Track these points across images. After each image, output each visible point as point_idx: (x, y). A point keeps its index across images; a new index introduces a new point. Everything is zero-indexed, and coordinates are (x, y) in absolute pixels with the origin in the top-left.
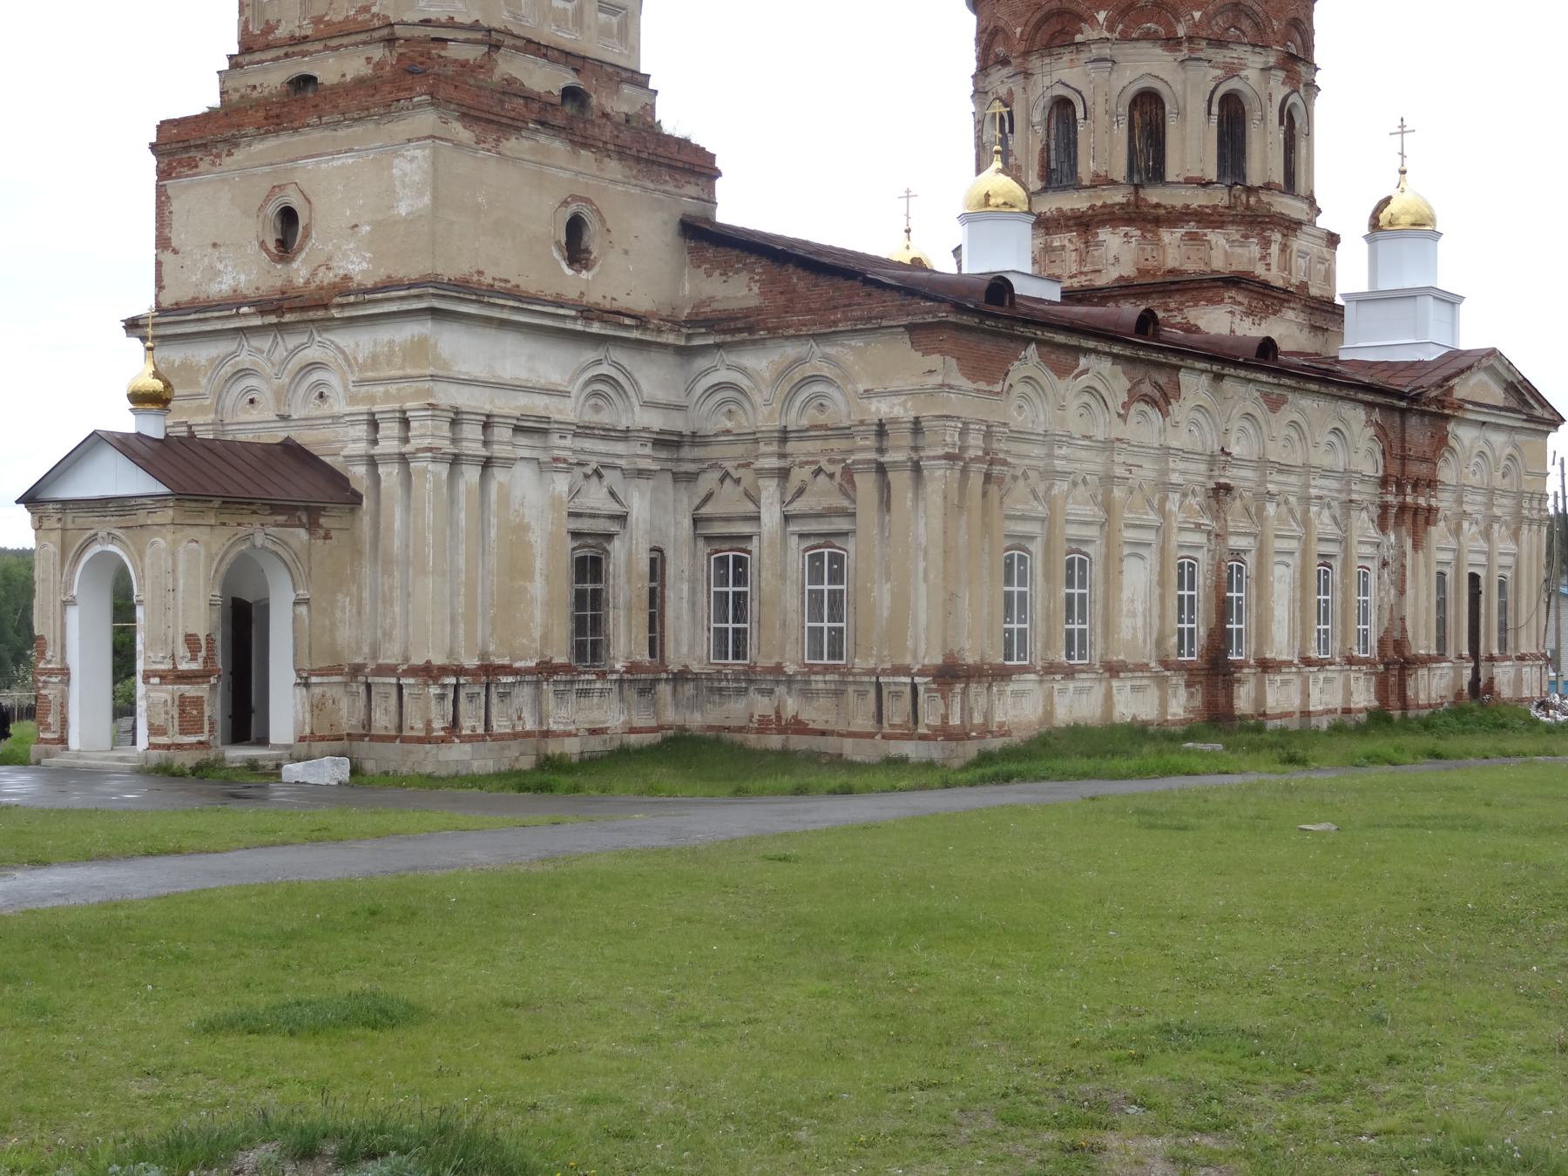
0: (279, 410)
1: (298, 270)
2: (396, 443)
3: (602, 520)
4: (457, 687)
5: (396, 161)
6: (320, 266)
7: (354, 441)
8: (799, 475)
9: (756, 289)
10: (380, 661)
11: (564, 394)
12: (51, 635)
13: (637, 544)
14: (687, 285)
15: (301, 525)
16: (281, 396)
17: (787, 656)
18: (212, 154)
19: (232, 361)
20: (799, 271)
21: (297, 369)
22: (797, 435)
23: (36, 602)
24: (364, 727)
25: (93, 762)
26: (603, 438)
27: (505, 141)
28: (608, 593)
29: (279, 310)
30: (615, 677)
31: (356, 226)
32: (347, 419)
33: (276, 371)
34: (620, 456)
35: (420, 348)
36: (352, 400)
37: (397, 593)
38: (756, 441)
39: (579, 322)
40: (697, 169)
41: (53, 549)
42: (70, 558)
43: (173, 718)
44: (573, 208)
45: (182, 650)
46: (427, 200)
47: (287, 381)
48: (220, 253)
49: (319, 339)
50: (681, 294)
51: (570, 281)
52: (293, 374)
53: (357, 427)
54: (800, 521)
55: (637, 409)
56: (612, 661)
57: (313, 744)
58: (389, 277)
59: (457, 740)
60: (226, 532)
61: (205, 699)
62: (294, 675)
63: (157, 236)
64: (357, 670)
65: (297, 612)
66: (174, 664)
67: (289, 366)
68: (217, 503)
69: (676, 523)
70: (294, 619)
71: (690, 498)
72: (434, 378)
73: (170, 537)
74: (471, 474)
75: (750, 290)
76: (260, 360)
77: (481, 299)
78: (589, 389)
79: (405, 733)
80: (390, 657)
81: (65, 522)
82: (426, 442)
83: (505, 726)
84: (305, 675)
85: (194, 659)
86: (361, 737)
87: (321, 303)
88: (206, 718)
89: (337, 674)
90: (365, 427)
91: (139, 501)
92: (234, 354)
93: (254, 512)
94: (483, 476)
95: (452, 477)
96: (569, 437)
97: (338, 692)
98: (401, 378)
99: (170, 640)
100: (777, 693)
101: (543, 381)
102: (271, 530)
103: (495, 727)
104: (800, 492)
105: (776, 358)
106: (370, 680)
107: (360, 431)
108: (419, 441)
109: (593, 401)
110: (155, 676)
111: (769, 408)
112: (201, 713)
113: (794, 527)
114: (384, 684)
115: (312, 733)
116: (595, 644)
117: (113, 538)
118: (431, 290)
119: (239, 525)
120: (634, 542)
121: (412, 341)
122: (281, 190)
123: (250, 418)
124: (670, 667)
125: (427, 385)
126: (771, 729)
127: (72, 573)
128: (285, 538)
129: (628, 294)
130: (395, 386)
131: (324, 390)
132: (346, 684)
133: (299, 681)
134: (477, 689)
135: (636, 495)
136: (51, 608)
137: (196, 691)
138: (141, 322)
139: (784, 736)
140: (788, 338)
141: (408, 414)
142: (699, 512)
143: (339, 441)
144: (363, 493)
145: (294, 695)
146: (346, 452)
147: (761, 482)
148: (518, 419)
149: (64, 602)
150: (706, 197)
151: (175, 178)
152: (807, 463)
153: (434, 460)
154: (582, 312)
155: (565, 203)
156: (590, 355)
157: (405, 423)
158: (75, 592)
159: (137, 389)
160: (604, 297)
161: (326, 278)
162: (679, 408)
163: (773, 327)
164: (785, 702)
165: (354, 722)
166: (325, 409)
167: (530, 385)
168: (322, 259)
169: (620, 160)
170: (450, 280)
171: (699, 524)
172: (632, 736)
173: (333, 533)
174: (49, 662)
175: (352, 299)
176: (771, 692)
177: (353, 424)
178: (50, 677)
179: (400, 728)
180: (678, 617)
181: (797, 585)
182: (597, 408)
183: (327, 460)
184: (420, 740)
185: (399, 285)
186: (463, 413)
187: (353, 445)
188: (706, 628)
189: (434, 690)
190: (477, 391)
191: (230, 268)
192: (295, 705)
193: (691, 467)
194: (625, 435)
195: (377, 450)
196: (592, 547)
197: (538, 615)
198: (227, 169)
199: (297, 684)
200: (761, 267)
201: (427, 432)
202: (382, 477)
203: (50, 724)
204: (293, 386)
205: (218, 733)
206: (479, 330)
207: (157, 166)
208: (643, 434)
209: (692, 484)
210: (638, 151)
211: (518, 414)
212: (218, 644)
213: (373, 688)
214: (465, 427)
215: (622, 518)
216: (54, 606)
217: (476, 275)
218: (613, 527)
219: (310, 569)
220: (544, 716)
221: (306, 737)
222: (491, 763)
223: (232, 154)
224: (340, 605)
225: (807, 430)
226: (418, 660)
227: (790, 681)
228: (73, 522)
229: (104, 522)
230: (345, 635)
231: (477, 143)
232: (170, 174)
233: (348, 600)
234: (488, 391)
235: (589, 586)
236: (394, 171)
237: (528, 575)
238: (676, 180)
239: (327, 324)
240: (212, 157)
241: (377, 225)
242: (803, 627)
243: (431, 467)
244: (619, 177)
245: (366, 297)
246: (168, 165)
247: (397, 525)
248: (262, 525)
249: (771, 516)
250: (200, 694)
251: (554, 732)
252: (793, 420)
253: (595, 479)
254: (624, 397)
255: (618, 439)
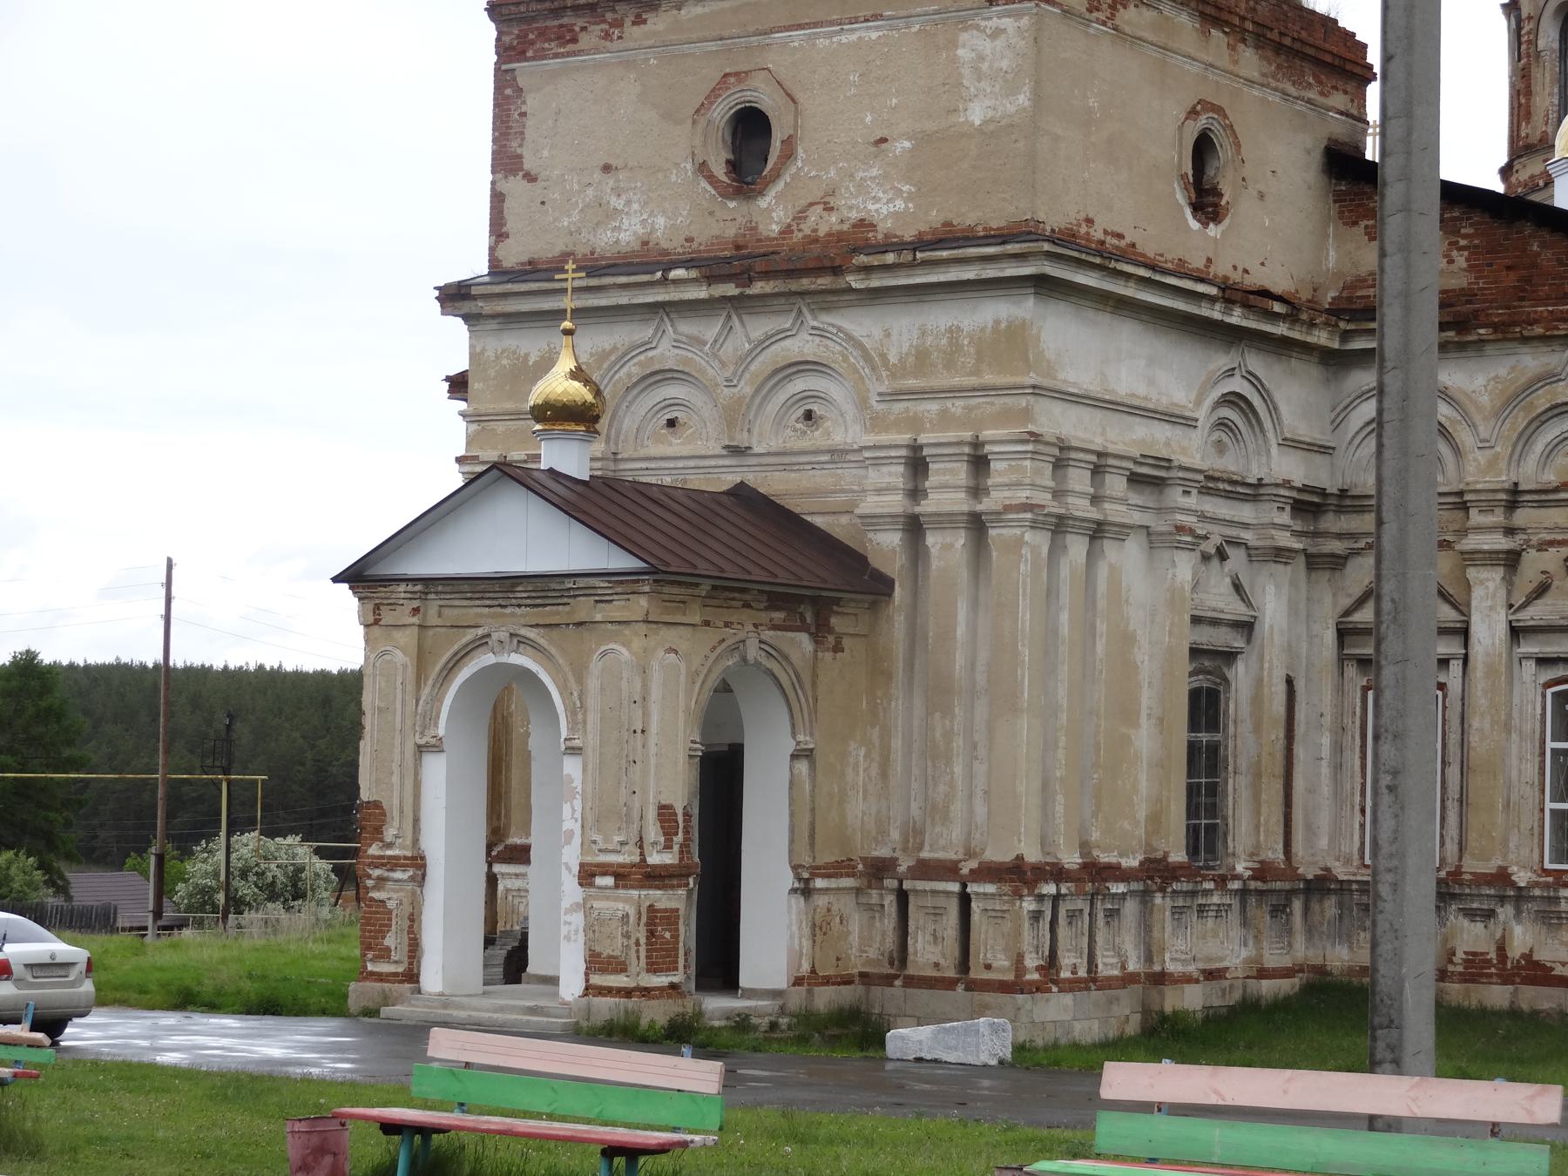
0: (732, 439)
1: (769, 210)
2: (963, 495)
3: (1224, 630)
4: (1057, 898)
5: (964, 37)
6: (811, 204)
7: (879, 491)
8: (1534, 565)
9: (1461, 260)
10: (925, 854)
11: (1188, 422)
12: (396, 802)
13: (1270, 669)
14: (1332, 253)
15: (803, 628)
16: (733, 415)
17: (1511, 856)
18: (604, 21)
19: (642, 357)
20: (1546, 235)
21: (770, 369)
22: (1536, 497)
23: (365, 747)
24: (891, 964)
25: (487, 1015)
26: (1228, 496)
27: (1122, 10)
28: (1226, 747)
29: (744, 276)
30: (1236, 885)
31: (884, 140)
32: (867, 454)
33: (728, 374)
34: (1246, 526)
35: (1014, 340)
36: (876, 423)
37: (959, 743)
38: (1464, 507)
39: (1218, 306)
40: (1349, 67)
41: (401, 658)
42: (433, 675)
43: (637, 944)
44: (1202, 122)
45: (653, 833)
46: (1023, 99)
47: (748, 390)
48: (618, 181)
49: (815, 324)
50: (1324, 268)
52: (761, 378)
53: (885, 469)
54: (1540, 637)
55: (1274, 450)
56: (1230, 860)
57: (817, 989)
58: (947, 224)
59: (1055, 989)
60: (711, 636)
61: (681, 913)
62: (790, 875)
63: (494, 153)
64: (879, 870)
65: (796, 772)
66: (642, 854)
67: (753, 368)
68: (705, 588)
69: (1311, 637)
70: (791, 783)
71: (1334, 595)
72: (1037, 390)
73: (637, 644)
74: (1077, 547)
75: (1451, 262)
76: (698, 359)
77: (1106, 263)
78: (1215, 417)
79: (972, 975)
80: (944, 849)
81: (425, 615)
82: (1022, 495)
83: (1111, 965)
84: (806, 875)
85: (668, 846)
86: (888, 980)
87: (827, 263)
88: (681, 944)
89: (848, 875)
90: (901, 469)
91: (582, 582)
92: (646, 346)
93: (747, 605)
94: (1092, 557)
95: (1056, 550)
96: (1194, 492)
97: (846, 904)
98: (974, 390)
99: (636, 816)
100: (1502, 917)
101: (1164, 400)
102: (768, 635)
103: (1100, 966)
104: (1542, 590)
105: (1502, 372)
106: (907, 885)
107: (890, 474)
108: (1007, 494)
109: (1217, 435)
110: (604, 874)
111: (1488, 453)
112: (675, 937)
113: (1530, 647)
114: (934, 892)
115: (813, 971)
116: (1211, 829)
117: (521, 642)
118: (1047, 247)
119: (727, 625)
120: (1266, 665)
121: (995, 329)
122: (740, 81)
123: (669, 451)
124: (1300, 871)
125: (1023, 401)
126: (1490, 975)
127: (437, 699)
128: (786, 649)
129: (1263, 264)
130: (960, 403)
131: (815, 407)
132: (858, 891)
133: (797, 885)
135: (1271, 589)
136: (397, 757)
137: (670, 899)
138: (474, 291)
139: (1511, 988)
140: (1525, 340)
141: (926, 452)
142: (1350, 619)
143: (843, 491)
144: (895, 576)
145: (789, 901)
146: (864, 509)
147: (1472, 573)
148: (1136, 462)
149: (419, 746)
150: (1355, 112)
151: (533, 59)
152: (1552, 543)
153: (1035, 525)
154: (1223, 290)
155: (1193, 113)
156: (1222, 360)
157: (979, 462)
158: (441, 732)
159: (552, 397)
160: (1235, 268)
161: (823, 223)
162: (1325, 450)
163: (1503, 324)
164: (1512, 931)
165: (872, 953)
166: (816, 439)
167: (1151, 406)
168: (817, 194)
169: (1257, 47)
170: (1053, 231)
171: (1348, 639)
172: (1265, 983)
173: (846, 642)
174: (390, 845)
175: (890, 258)
176: (1489, 914)
177: (877, 462)
178: (391, 870)
179: (964, 964)
180: (1312, 790)
181: (1532, 742)
182: (1220, 447)
183: (818, 521)
184: (1005, 988)
185: (967, 238)
186: (1070, 448)
187: (877, 498)
188: (1357, 808)
189: (1029, 905)
190: (1086, 414)
191: (636, 206)
192: (791, 924)
193: (1337, 547)
194: (1254, 492)
195: (985, 505)
196: (1209, 673)
197: (1144, 782)
198: (632, 45)
199: (794, 891)
200: (1471, 225)
202: (932, 550)
203: (388, 949)
204: (758, 400)
205: (693, 971)
206: (1091, 314)
207: (498, 40)
208: (1282, 492)
209: (1337, 574)
210: (1281, 34)
211: (1135, 453)
212: (695, 821)
213: (912, 899)
214: (1108, 476)
215: (1246, 627)
216: (402, 753)
217: (1084, 225)
218: (1239, 643)
219: (816, 700)
220: (1154, 949)
221: (802, 978)
222: (1096, 1025)
223: (645, 22)
224: (851, 760)
225: (1556, 490)
226: (998, 854)
227: (1521, 897)
228: (440, 616)
229: (504, 615)
230: (858, 810)
231: (1090, 11)
232: (524, 52)
233: (863, 751)
234: (1099, 414)
235: (1204, 737)
236: (960, 52)
238: (1320, 82)
239: (828, 300)
240: (605, 26)
241: (923, 140)
242: (1542, 810)
243: (1028, 536)
244: (1256, 75)
245: (919, 255)
246: (518, 37)
247: (961, 630)
248: (755, 626)
249: (1489, 630)
250: (673, 905)
251: (1171, 974)
252: (1530, 473)
253: (1215, 562)
254: (1257, 429)
255: (1244, 498)
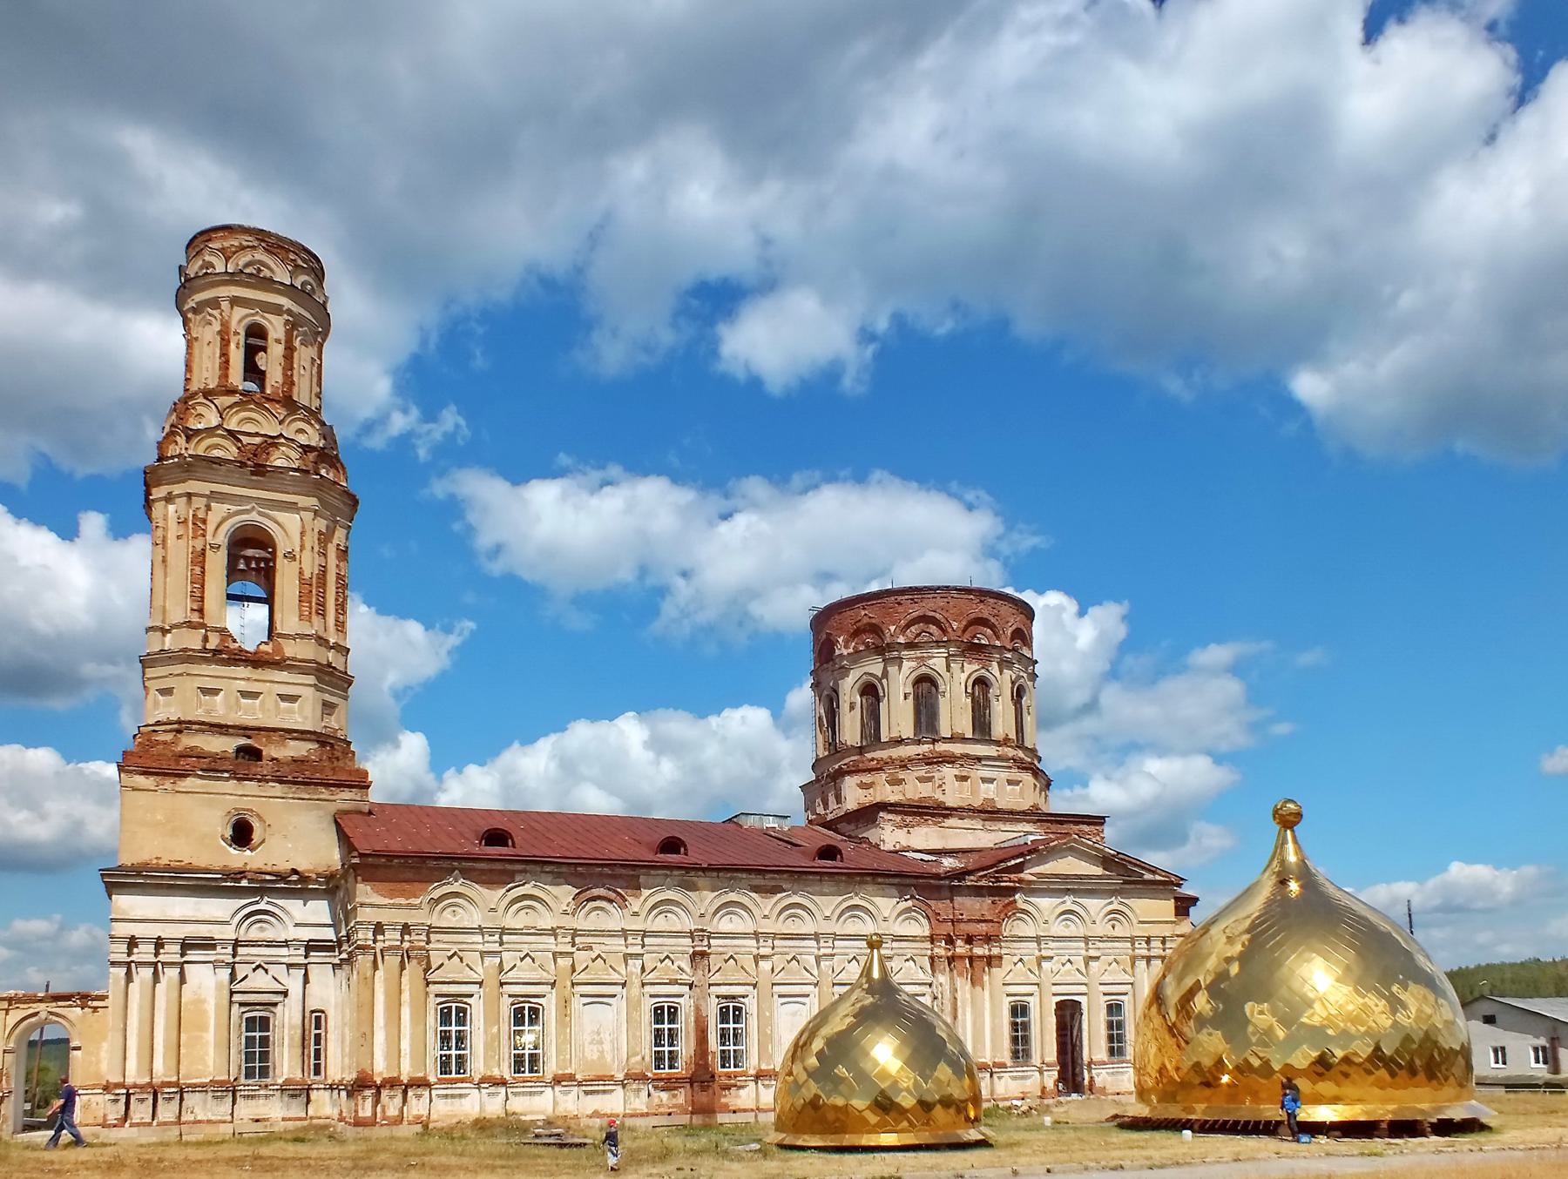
51: (237, 858)
134: (145, 1096)
194: (286, 944)
201: (119, 952)
215: (285, 994)
237: (205, 1028)
